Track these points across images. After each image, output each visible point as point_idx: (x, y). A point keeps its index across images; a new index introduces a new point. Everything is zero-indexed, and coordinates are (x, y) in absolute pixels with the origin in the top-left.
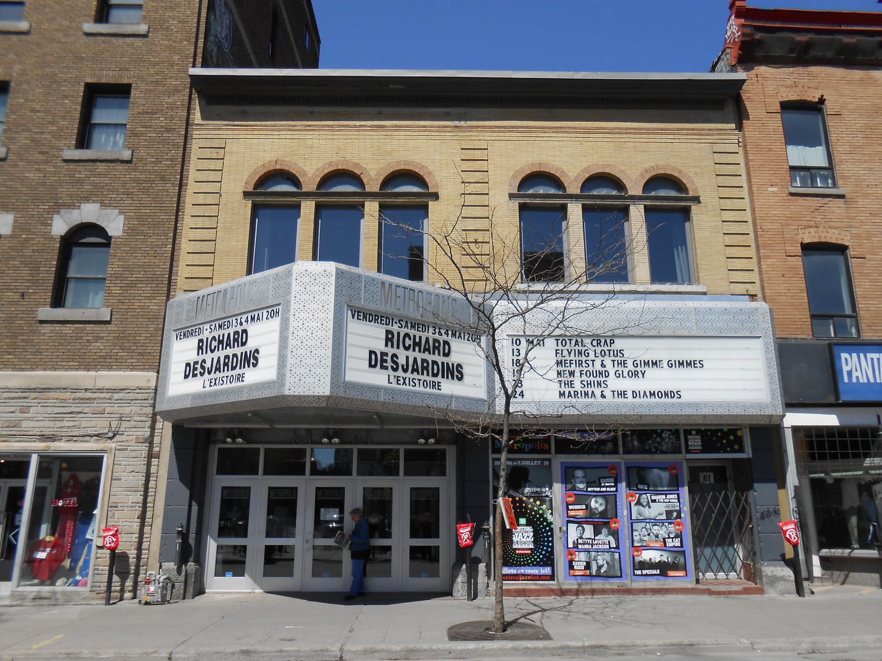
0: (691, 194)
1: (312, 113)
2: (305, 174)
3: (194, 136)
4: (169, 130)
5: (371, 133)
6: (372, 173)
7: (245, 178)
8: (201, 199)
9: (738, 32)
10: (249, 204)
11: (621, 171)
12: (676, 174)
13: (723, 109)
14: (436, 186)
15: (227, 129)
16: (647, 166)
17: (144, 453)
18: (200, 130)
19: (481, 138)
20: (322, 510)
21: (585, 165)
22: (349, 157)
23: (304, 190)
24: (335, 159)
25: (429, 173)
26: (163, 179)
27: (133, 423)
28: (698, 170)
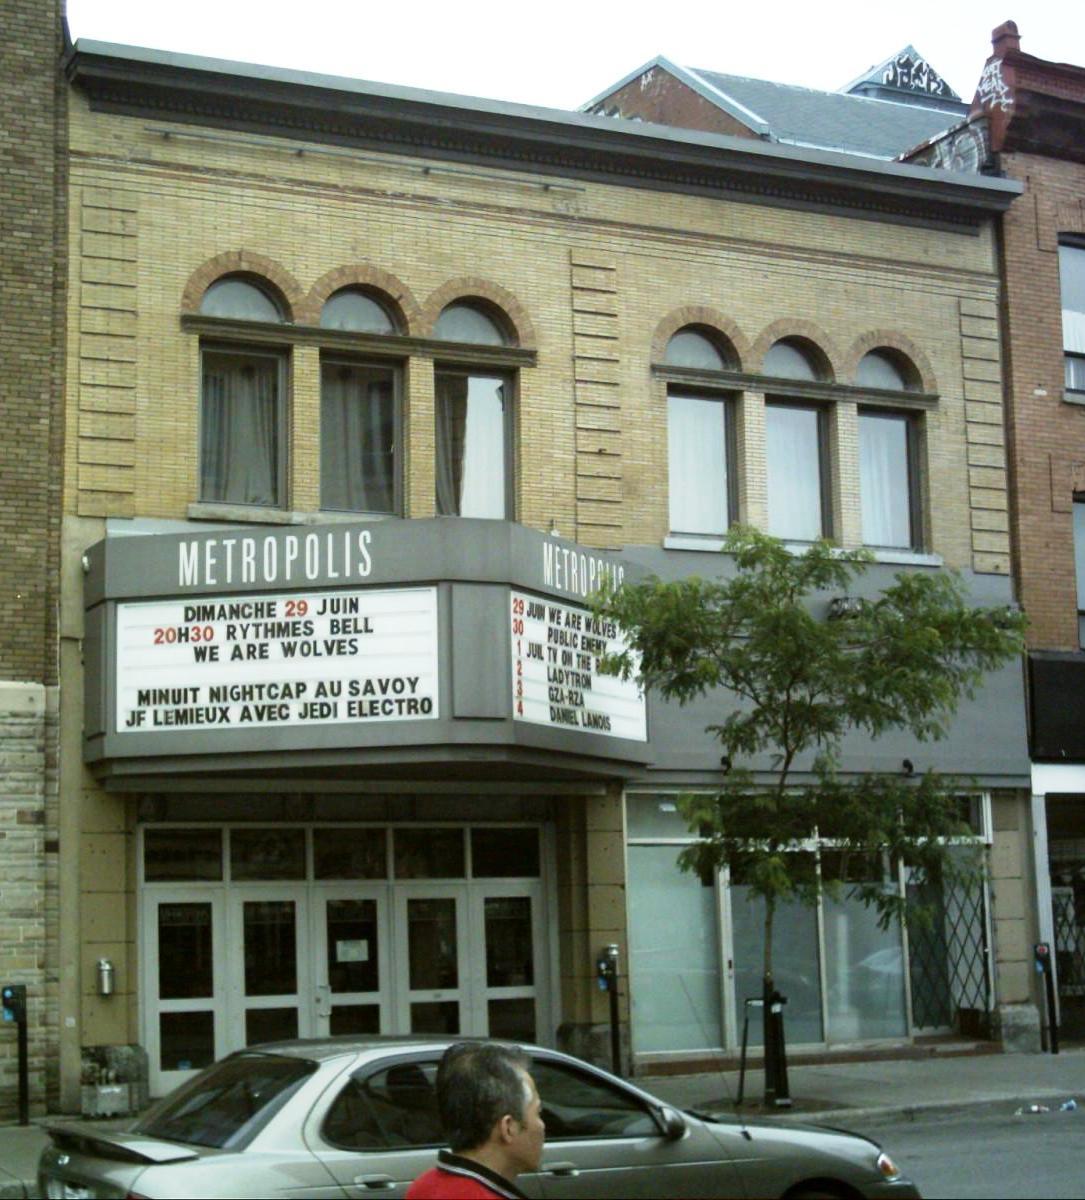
0: (927, 391)
1: (300, 154)
2: (297, 289)
3: (72, 179)
4: (22, 160)
5: (412, 213)
6: (420, 299)
7: (182, 286)
8: (98, 321)
9: (1008, 95)
10: (194, 340)
11: (825, 336)
12: (905, 350)
13: (977, 236)
14: (532, 336)
15: (140, 172)
16: (862, 331)
17: (37, 844)
18: (83, 166)
19: (604, 246)
20: (340, 945)
21: (771, 318)
22: (376, 261)
23: (298, 322)
24: (352, 262)
25: (519, 309)
26: (18, 269)
27: (13, 784)
28: (939, 345)
